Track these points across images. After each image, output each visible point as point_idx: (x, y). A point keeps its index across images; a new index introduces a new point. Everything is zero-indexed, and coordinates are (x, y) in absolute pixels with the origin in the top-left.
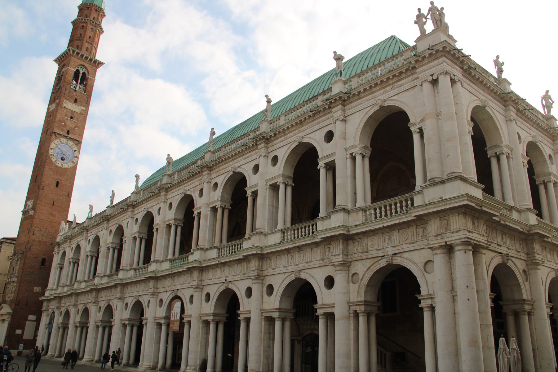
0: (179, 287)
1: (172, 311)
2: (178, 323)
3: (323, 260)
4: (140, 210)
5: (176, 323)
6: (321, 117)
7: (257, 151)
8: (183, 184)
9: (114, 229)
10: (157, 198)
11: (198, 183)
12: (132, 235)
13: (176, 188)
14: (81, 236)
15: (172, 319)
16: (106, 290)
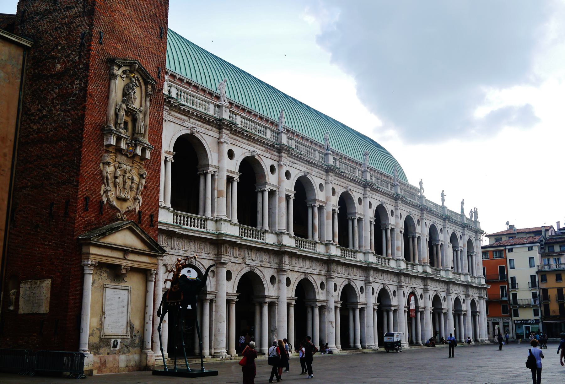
0: (414, 286)
1: (410, 303)
2: (414, 311)
3: (463, 292)
4: (374, 196)
5: (413, 311)
6: (460, 227)
7: (443, 221)
8: (409, 206)
9: (340, 191)
10: (391, 200)
11: (417, 213)
12: (370, 218)
13: (404, 204)
14: (264, 149)
15: (410, 308)
16: (342, 267)
